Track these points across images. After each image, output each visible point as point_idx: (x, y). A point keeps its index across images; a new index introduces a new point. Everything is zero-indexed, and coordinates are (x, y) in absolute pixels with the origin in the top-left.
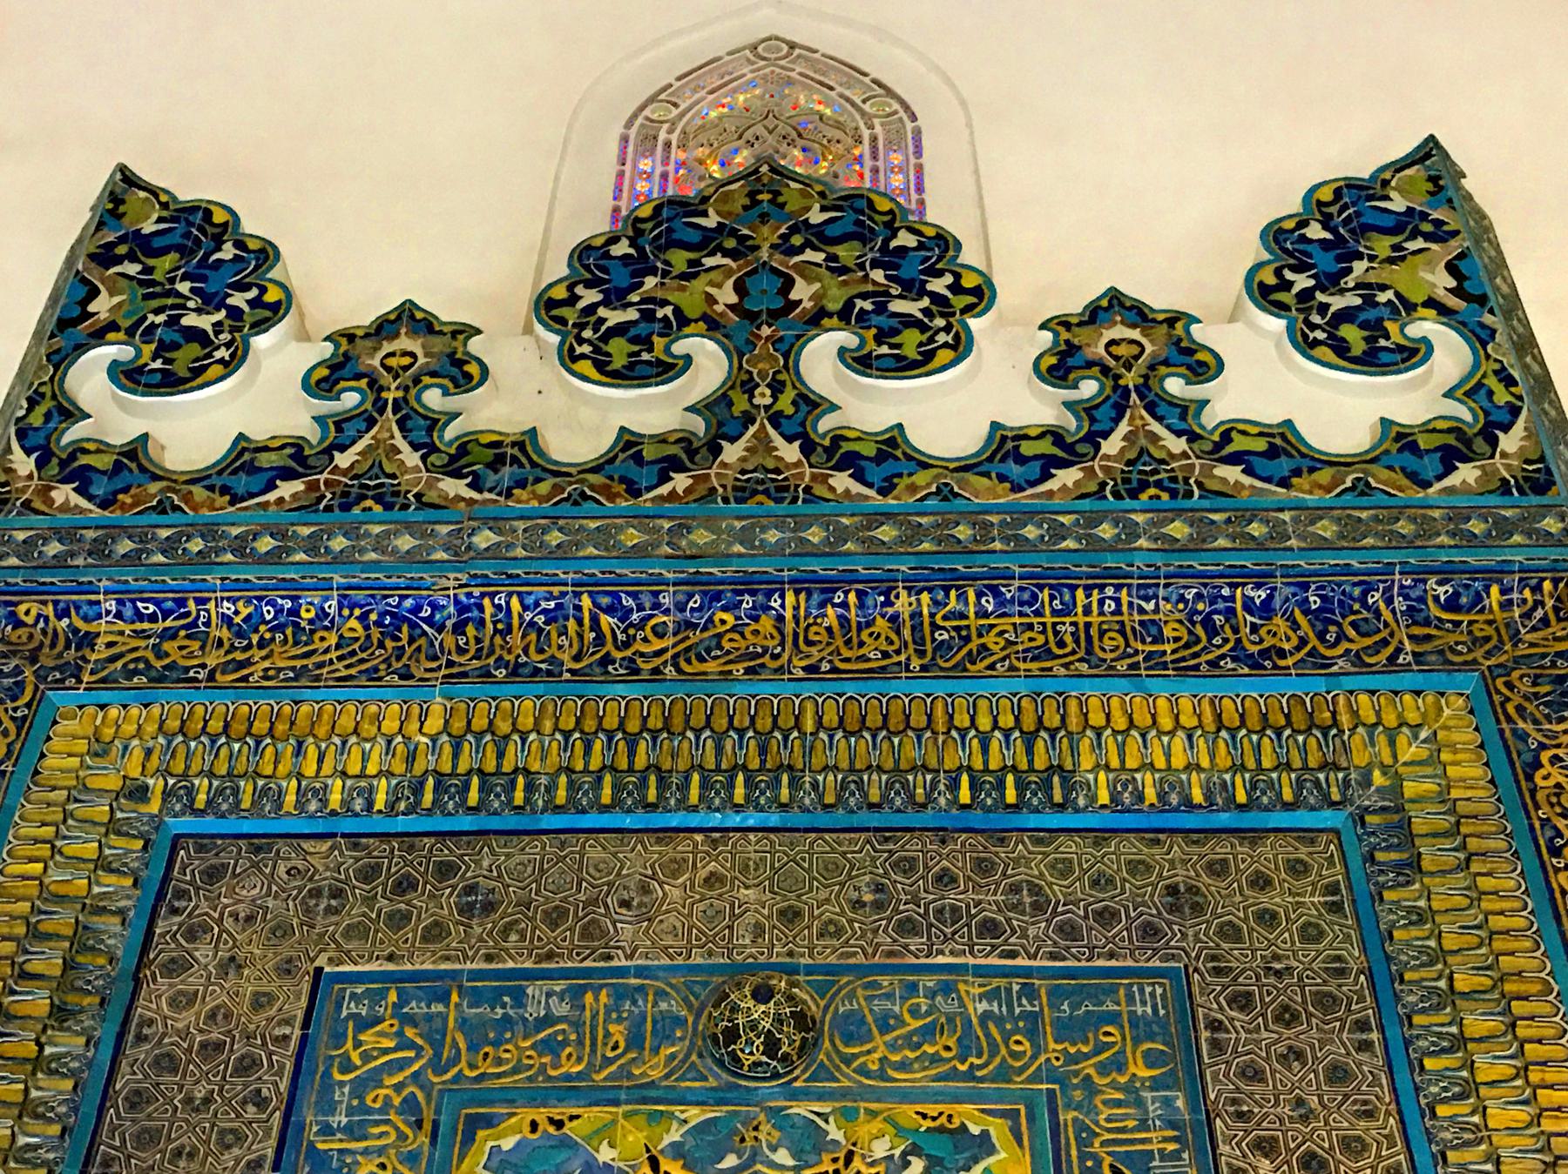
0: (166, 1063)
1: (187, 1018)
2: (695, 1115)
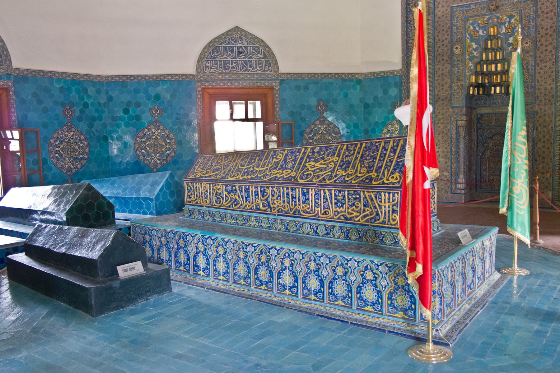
0: (439, 18)
1: (440, 13)
2: (487, 17)
